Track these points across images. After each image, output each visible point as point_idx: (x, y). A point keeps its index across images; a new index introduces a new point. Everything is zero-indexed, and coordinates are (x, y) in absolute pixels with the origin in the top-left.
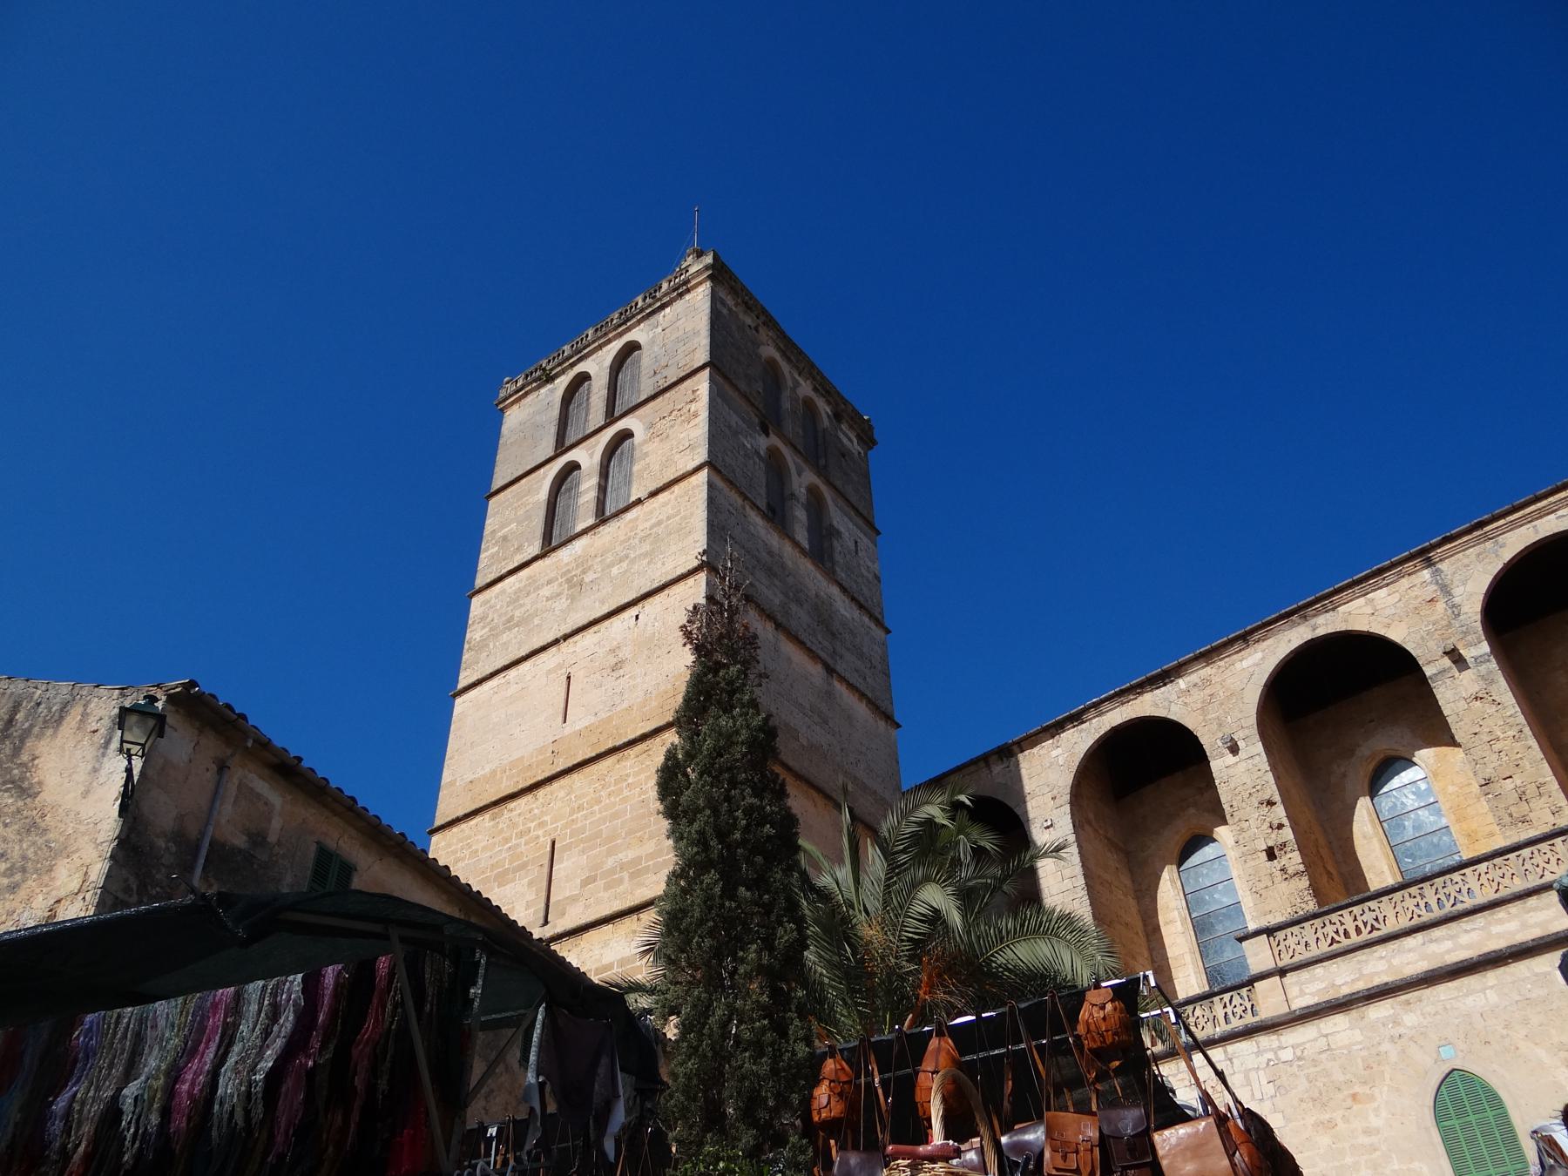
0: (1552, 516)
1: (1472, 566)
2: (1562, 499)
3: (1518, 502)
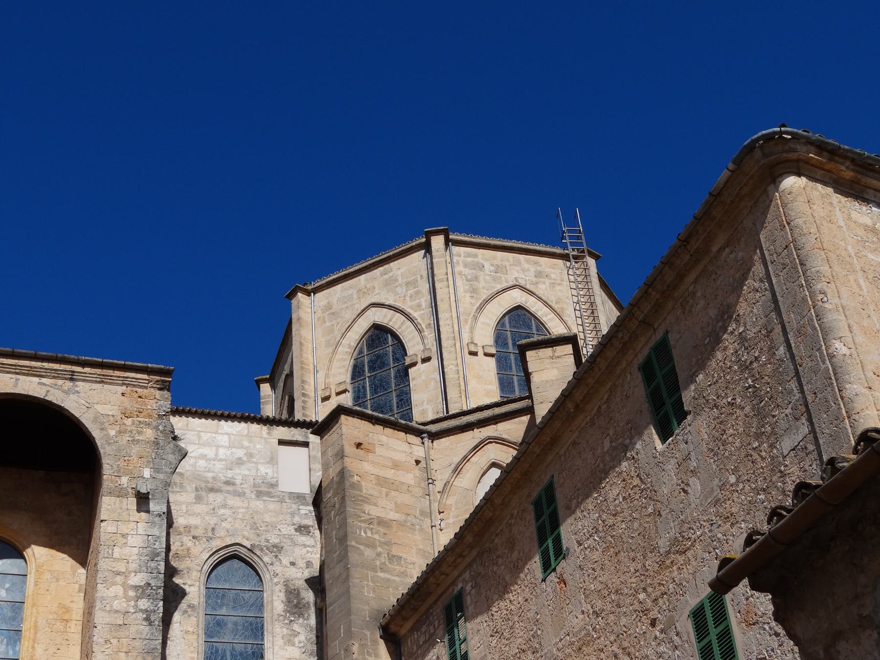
0: (36, 379)
2: (54, 370)
3: (19, 350)
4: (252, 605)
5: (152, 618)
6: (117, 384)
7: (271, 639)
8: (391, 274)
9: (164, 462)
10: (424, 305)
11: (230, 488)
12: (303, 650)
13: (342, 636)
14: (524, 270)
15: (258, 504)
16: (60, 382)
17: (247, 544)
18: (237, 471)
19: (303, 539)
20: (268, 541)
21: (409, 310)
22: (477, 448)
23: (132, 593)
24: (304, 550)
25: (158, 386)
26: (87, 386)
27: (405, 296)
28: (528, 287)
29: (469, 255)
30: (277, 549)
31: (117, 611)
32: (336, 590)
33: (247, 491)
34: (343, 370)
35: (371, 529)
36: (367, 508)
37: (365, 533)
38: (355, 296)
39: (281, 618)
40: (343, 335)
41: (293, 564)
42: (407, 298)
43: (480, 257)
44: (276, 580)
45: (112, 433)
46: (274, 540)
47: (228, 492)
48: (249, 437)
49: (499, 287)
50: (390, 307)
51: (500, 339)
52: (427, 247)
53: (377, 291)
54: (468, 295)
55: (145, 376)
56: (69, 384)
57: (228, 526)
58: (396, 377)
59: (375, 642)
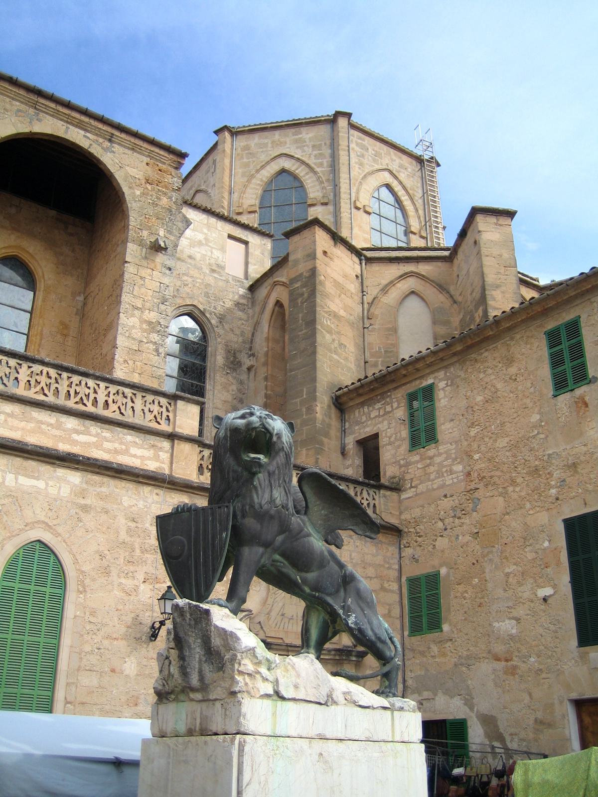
0: (82, 132)
1: (9, 113)
2: (98, 128)
4: (199, 355)
5: (160, 351)
6: (144, 155)
7: (212, 383)
9: (175, 227)
10: (325, 164)
12: (235, 397)
13: (305, 396)
14: (393, 160)
16: (101, 140)
17: (201, 307)
18: (197, 249)
23: (144, 326)
24: (240, 322)
25: (175, 166)
26: (121, 149)
27: (310, 154)
28: (394, 172)
29: (360, 138)
31: (134, 339)
32: (299, 361)
34: (254, 196)
35: (330, 320)
36: (329, 303)
37: (327, 321)
38: (270, 145)
42: (312, 156)
43: (366, 141)
45: (138, 193)
48: (209, 226)
49: (377, 167)
53: (288, 146)
55: (166, 155)
56: (107, 144)
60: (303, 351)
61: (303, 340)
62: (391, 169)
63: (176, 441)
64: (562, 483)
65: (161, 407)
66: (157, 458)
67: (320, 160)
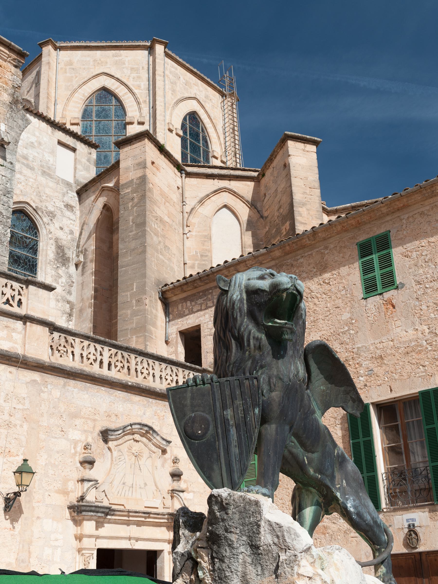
4: (31, 249)
7: (44, 275)
8: (120, 58)
11: (25, 162)
12: (64, 289)
13: (135, 290)
15: (42, 179)
19: (68, 213)
20: (47, 207)
21: (131, 87)
22: (216, 192)
24: (69, 222)
27: (129, 76)
28: (201, 101)
30: (52, 215)
32: (130, 258)
33: (36, 168)
34: (77, 110)
35: (157, 224)
37: (154, 225)
39: (52, 263)
40: (80, 86)
41: (61, 229)
42: (130, 78)
44: (50, 236)
46: (51, 208)
47: (23, 164)
49: (187, 95)
50: (118, 80)
51: (183, 126)
52: (151, 49)
53: (108, 66)
54: (170, 92)
57: (22, 188)
58: (116, 127)
59: (156, 300)
60: (133, 250)
61: (133, 240)
62: (199, 98)
63: (28, 324)
64: (370, 372)
65: (14, 290)
66: (10, 338)
67: (138, 83)
